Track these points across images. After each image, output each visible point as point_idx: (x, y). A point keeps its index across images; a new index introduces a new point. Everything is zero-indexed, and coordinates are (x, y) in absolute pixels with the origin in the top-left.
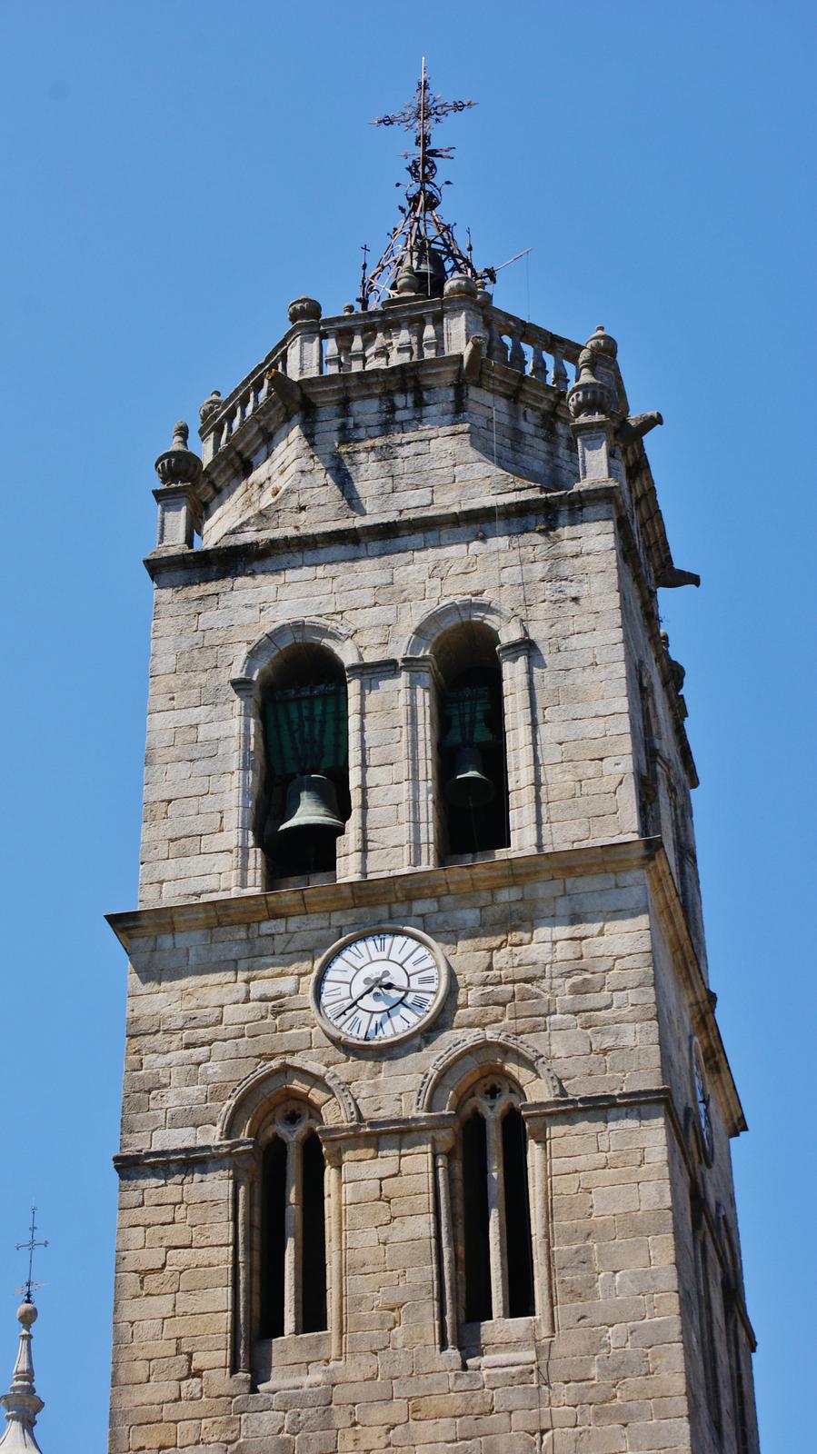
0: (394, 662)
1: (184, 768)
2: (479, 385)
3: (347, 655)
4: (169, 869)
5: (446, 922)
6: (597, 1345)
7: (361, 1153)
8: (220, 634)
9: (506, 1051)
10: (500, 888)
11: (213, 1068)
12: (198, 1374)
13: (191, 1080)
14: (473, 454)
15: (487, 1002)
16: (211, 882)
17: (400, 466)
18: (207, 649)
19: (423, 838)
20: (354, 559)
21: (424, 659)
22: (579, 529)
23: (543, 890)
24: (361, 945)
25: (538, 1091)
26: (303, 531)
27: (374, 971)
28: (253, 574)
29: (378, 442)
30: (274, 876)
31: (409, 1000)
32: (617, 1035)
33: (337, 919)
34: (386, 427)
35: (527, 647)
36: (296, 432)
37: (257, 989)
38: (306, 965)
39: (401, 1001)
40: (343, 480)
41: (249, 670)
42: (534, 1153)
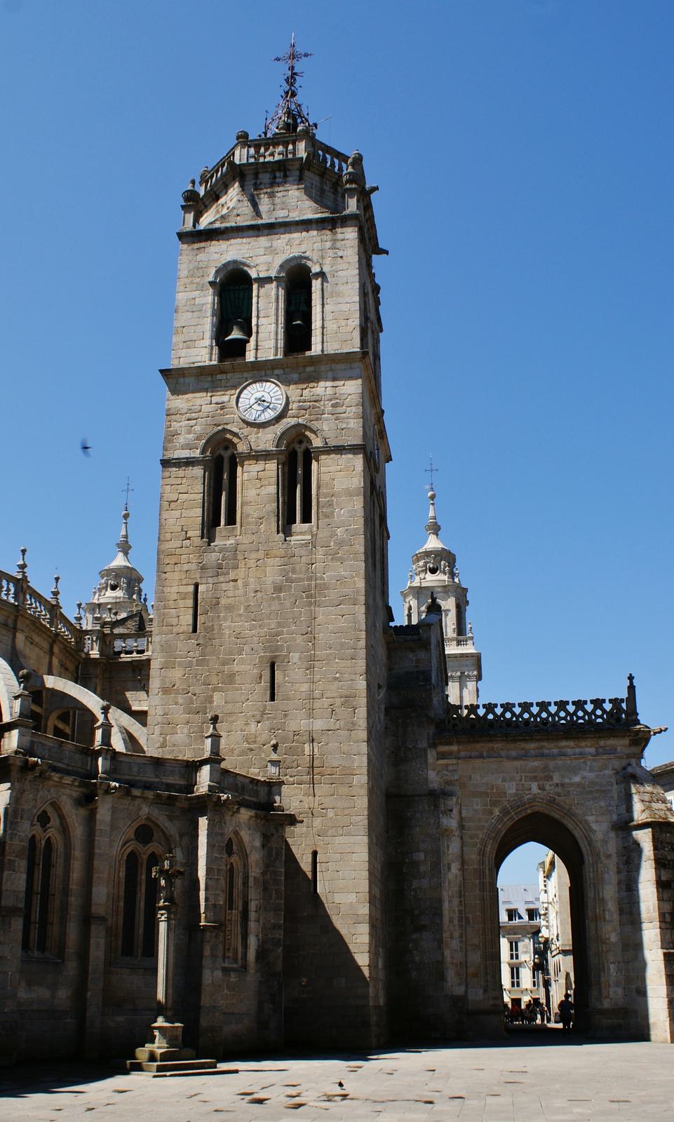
0: (271, 278)
1: (190, 315)
2: (309, 170)
3: (253, 274)
4: (183, 353)
5: (286, 378)
6: (333, 534)
7: (251, 462)
8: (205, 263)
9: (306, 427)
10: (307, 366)
11: (198, 428)
12: (189, 538)
13: (189, 433)
14: (305, 197)
15: (300, 408)
16: (199, 359)
17: (277, 200)
18: (199, 269)
19: (279, 346)
20: (257, 237)
21: (283, 277)
22: (344, 230)
23: (323, 368)
24: (254, 385)
25: (317, 442)
26: (238, 224)
27: (259, 395)
28: (218, 240)
29: (269, 190)
30: (222, 357)
31: (271, 406)
32: (347, 423)
33: (245, 375)
34: (272, 185)
35: (322, 274)
36: (237, 184)
37: (215, 399)
38: (233, 392)
39: (268, 407)
40: (255, 205)
41: (216, 279)
42: (314, 465)
